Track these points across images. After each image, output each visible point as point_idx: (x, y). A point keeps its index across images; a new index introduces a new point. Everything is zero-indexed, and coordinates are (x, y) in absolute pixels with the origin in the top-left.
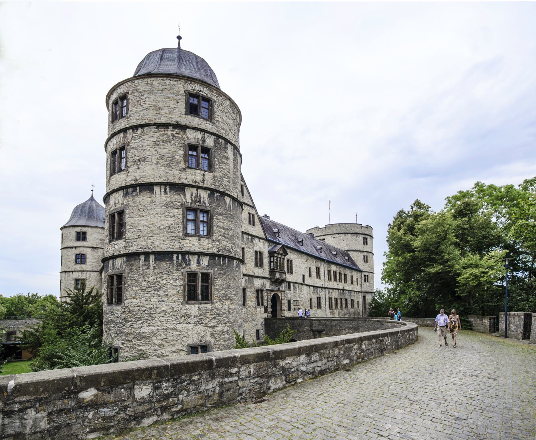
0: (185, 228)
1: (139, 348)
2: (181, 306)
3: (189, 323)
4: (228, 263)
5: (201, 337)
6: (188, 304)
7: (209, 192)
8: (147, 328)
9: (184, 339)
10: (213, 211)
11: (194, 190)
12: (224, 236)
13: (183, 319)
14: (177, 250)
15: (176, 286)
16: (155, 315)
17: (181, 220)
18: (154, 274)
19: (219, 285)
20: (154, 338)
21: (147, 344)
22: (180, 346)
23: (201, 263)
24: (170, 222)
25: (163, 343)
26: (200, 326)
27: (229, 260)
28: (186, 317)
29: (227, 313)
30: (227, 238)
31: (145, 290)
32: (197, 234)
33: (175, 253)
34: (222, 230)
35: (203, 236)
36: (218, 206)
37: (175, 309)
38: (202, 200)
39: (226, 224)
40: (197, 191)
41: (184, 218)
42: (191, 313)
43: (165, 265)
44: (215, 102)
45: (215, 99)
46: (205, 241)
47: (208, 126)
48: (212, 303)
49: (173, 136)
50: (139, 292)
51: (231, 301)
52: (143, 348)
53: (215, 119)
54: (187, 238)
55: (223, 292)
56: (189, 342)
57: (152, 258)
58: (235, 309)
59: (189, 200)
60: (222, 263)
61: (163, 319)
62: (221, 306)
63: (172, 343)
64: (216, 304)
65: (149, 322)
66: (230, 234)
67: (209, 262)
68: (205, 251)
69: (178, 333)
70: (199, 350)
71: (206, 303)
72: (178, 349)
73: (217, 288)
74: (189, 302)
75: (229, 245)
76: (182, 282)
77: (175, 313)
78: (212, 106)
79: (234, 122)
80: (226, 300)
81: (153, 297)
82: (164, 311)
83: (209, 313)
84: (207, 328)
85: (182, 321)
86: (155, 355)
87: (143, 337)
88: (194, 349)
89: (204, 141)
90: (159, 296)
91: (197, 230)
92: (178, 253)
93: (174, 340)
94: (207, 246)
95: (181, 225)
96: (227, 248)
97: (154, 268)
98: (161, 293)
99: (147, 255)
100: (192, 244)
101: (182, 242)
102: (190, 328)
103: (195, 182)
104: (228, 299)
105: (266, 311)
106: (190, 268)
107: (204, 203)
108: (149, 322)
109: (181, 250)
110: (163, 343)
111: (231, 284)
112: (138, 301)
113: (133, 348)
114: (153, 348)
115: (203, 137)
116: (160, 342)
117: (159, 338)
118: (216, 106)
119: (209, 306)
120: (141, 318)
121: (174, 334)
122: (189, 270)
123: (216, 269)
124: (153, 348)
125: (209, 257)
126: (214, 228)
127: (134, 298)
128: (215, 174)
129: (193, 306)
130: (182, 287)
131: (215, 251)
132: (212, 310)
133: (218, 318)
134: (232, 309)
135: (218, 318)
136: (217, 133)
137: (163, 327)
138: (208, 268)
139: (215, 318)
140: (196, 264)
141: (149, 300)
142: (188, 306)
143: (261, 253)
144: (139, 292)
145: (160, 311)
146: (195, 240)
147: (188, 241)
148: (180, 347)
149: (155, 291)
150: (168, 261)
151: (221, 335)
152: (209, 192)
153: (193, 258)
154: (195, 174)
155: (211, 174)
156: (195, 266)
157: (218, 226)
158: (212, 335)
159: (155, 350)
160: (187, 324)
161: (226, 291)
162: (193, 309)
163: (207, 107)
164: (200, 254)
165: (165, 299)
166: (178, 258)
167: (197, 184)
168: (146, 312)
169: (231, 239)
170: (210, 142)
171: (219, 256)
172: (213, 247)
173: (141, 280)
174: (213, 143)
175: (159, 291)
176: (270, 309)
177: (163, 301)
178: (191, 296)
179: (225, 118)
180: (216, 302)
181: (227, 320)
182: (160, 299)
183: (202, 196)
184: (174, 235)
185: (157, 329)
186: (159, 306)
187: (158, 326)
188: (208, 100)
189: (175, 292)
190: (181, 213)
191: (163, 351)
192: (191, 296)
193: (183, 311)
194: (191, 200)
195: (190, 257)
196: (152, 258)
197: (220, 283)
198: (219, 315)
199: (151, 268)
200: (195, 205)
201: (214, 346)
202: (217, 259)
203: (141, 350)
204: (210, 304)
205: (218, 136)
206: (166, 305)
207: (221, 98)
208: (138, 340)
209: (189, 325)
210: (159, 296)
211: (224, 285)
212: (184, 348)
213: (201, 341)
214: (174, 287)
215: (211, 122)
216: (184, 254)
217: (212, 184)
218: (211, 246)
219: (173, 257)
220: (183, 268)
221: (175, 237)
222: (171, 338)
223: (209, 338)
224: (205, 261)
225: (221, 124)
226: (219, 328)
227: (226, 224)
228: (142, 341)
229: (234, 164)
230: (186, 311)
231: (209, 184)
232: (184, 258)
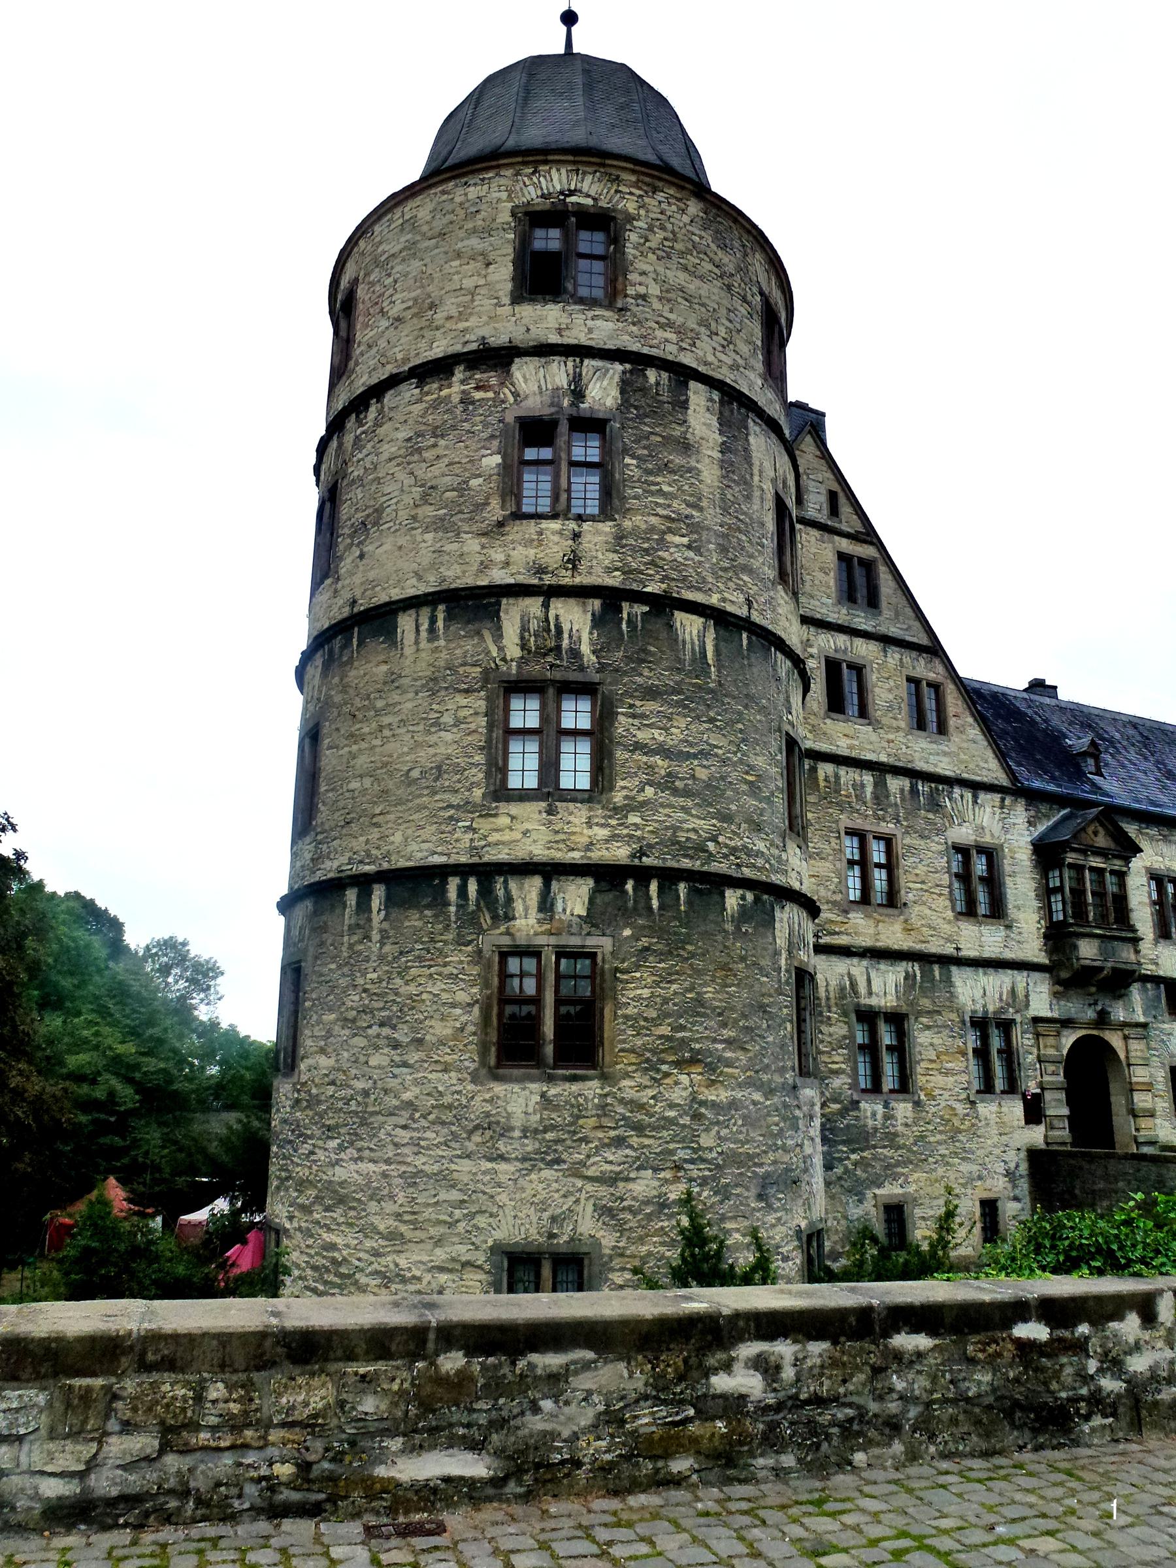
0: (498, 768)
1: (328, 1237)
2: (471, 1087)
3: (502, 1158)
4: (689, 902)
5: (553, 1219)
6: (497, 1078)
7: (596, 604)
8: (353, 1167)
9: (481, 1221)
10: (615, 682)
11: (533, 605)
12: (667, 784)
13: (476, 1138)
14: (463, 859)
15: (454, 1005)
16: (380, 1118)
17: (479, 739)
18: (382, 958)
19: (639, 998)
20: (373, 1206)
21: (351, 1225)
22: (463, 1249)
23: (559, 906)
24: (442, 750)
25: (403, 1228)
26: (547, 1173)
27: (692, 891)
28: (488, 1133)
29: (686, 1120)
30: (687, 793)
31: (354, 1021)
32: (549, 790)
33: (454, 874)
34: (658, 760)
35: (573, 796)
36: (640, 658)
37: (447, 1100)
38: (565, 643)
39: (679, 731)
40: (546, 605)
41: (490, 726)
42: (509, 1116)
43: (418, 924)
44: (630, 218)
45: (631, 207)
46: (576, 816)
47: (600, 328)
48: (605, 1078)
49: (466, 400)
50: (337, 1029)
51: (711, 1068)
52: (339, 1240)
53: (631, 291)
54: (504, 807)
55: (665, 1030)
56: (498, 1235)
57: (378, 894)
58: (733, 1104)
59: (514, 651)
60: (655, 903)
61: (404, 1136)
62: (651, 1092)
63: (433, 1231)
64: (626, 1083)
65: (360, 1144)
66: (702, 774)
67: (591, 900)
68: (576, 856)
69: (455, 1195)
70: (546, 1271)
71: (574, 1079)
72: (453, 1260)
73: (630, 1011)
74: (501, 1071)
75: (697, 824)
76: (475, 990)
77: (448, 1114)
78: (616, 240)
79: (729, 287)
80: (678, 1064)
81: (377, 1048)
82: (409, 1104)
83: (592, 1122)
84: (579, 1183)
85: (470, 1146)
86: (376, 1273)
87: (342, 1200)
88: (520, 1267)
89: (578, 394)
90: (396, 1045)
91: (549, 767)
92: (463, 871)
93: (440, 1222)
94: (590, 835)
95: (479, 758)
96: (682, 836)
97: (384, 937)
98: (402, 1035)
99: (364, 882)
100: (523, 833)
101: (483, 825)
102: (503, 1178)
103: (541, 570)
104: (693, 1061)
105: (1034, 1112)
106: (507, 933)
107: (575, 654)
108: (360, 1144)
109: (476, 860)
110: (403, 1228)
111: (709, 992)
112: (331, 1062)
113: (312, 1236)
114: (368, 1244)
115: (577, 379)
116: (391, 1222)
117: (389, 1207)
118: (633, 237)
119: (592, 1088)
120: (337, 1126)
121: (443, 1195)
122: (506, 941)
123: (627, 932)
124: (368, 1244)
125: (591, 882)
126: (620, 754)
127: (322, 1051)
128: (627, 524)
129: (516, 1088)
130: (476, 1010)
131: (620, 853)
132: (603, 1106)
133: (635, 1141)
134: (714, 1105)
135: (635, 1141)
136: (635, 347)
137: (403, 1168)
138: (586, 928)
139: (619, 1142)
140: (534, 914)
141: (362, 1059)
142: (499, 1088)
143: (991, 854)
144: (337, 1029)
145: (395, 1102)
146: (532, 812)
147: (504, 821)
148: (463, 1251)
149: (382, 1025)
150: (428, 907)
151: (649, 1217)
152: (597, 603)
153: (521, 889)
154: (539, 541)
155: (607, 527)
156: (532, 921)
157: (638, 747)
158: (605, 1212)
159: (376, 1254)
160: (491, 1160)
161: (682, 1028)
162: (520, 1099)
163: (599, 250)
164: (551, 872)
165: (414, 1057)
166: (462, 892)
167: (548, 580)
168: (353, 1106)
169: (708, 795)
170: (603, 391)
171: (643, 875)
172: (614, 837)
173: (343, 982)
174: (615, 392)
175: (394, 1027)
176: (1057, 1107)
177: (405, 1064)
178: (513, 1042)
179: (678, 277)
180: (627, 1075)
181: (682, 1154)
182: (397, 1059)
183: (566, 627)
184: (455, 800)
185: (385, 1175)
186: (392, 1083)
187: (388, 1162)
188: (602, 221)
189: (449, 1031)
190: (481, 705)
191: (403, 1263)
192: (513, 1042)
193: (479, 1106)
194: (523, 646)
195: (513, 885)
196: (378, 894)
197: (646, 993)
198: (639, 1128)
199: (376, 936)
200: (535, 669)
201: (616, 1263)
202: (629, 886)
203: (333, 1247)
204: (595, 1084)
205: (638, 361)
206: (416, 1082)
207: (660, 196)
208: (328, 1209)
209: (503, 1166)
210: (396, 1045)
211: (666, 1001)
212: (481, 1258)
213: (552, 1236)
214: (446, 1010)
215: (610, 306)
216: (487, 873)
217: (609, 570)
218: (603, 833)
219: (443, 890)
220: (481, 931)
221: (458, 807)
222: (429, 1213)
223: (587, 1225)
224: (574, 898)
225: (656, 305)
226: (644, 1185)
227: (679, 731)
228: (337, 1214)
229: (727, 467)
230: (488, 1107)
231: (599, 570)
232: (485, 891)
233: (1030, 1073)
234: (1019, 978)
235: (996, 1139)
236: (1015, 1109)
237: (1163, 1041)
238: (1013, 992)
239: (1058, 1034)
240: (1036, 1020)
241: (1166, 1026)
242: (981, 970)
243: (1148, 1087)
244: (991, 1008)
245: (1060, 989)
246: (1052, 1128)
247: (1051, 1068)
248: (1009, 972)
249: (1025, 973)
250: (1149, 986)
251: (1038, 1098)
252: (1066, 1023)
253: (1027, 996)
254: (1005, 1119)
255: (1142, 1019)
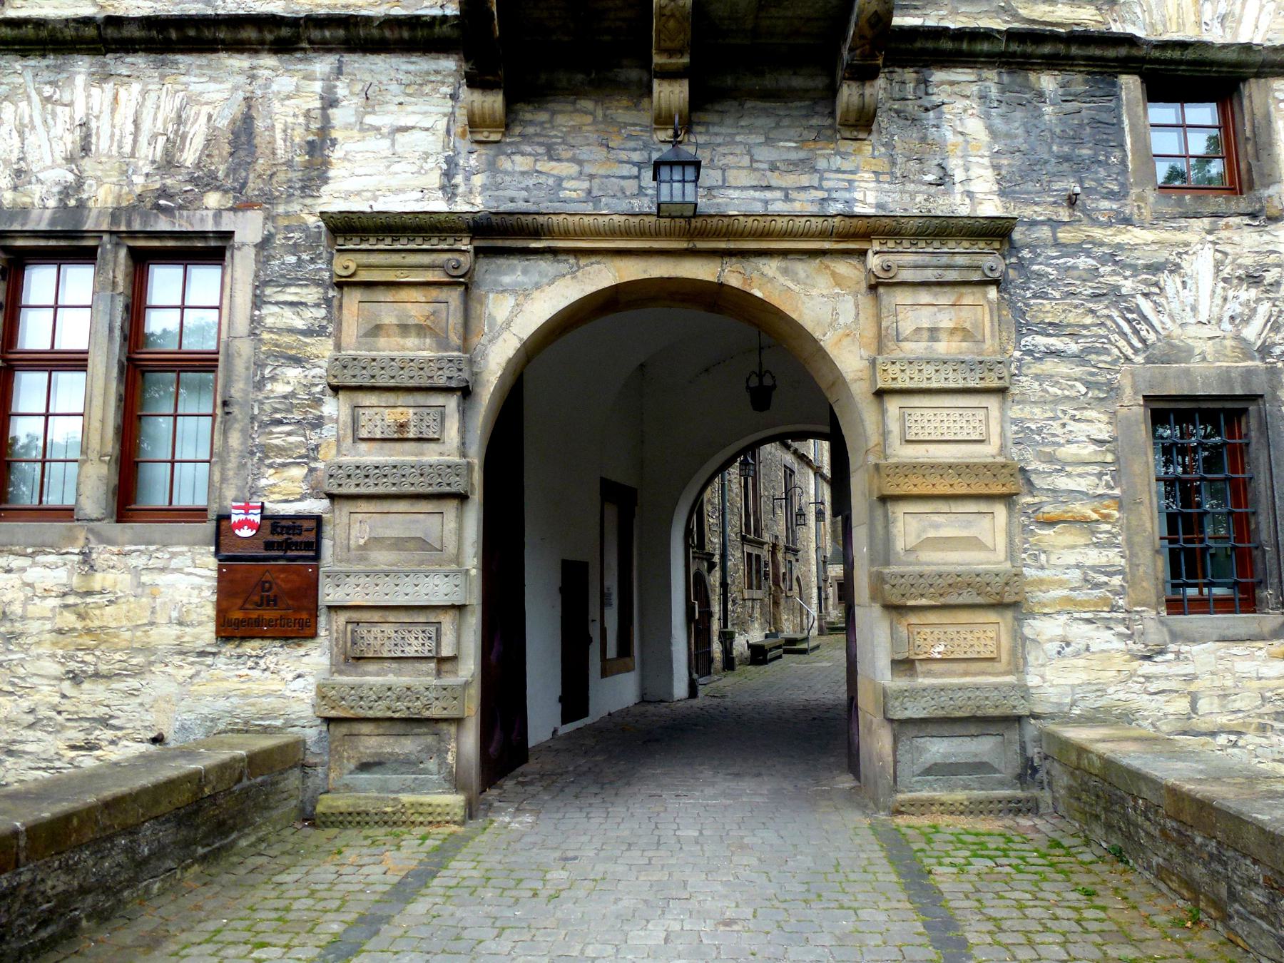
105: (269, 586)
233: (278, 437)
234: (284, 83)
235: (46, 694)
236: (186, 580)
237: (1115, 296)
238: (244, 133)
239: (465, 284)
240: (345, 227)
241: (1135, 235)
242: (82, 66)
243: (1003, 486)
244: (102, 196)
245: (493, 102)
246: (354, 658)
247: (383, 414)
248: (239, 62)
249: (323, 65)
250: (1048, 82)
251: (295, 539)
252: (505, 235)
253: (318, 148)
254: (108, 616)
255: (991, 208)
